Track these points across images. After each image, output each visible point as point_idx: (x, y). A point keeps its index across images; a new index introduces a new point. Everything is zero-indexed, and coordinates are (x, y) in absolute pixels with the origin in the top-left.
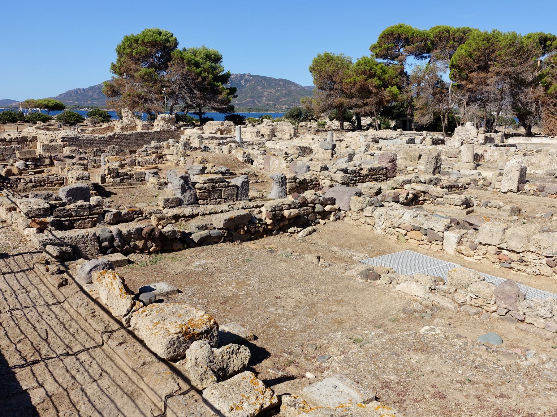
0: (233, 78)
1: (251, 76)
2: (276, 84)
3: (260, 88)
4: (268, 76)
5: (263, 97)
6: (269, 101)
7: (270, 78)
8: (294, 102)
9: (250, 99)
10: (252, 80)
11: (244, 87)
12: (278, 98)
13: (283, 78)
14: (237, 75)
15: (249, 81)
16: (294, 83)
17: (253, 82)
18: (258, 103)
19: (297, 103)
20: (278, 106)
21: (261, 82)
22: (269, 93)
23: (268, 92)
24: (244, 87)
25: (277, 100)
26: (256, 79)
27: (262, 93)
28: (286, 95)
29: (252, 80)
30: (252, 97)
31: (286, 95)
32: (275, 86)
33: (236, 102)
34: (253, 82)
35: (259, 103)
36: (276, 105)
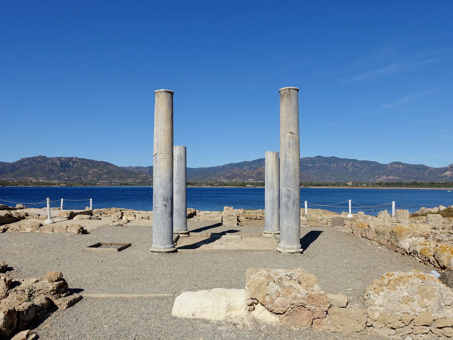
0: (63, 160)
1: (78, 159)
2: (98, 165)
3: (85, 168)
6: (93, 178)
7: (93, 161)
8: (114, 178)
9: (78, 176)
10: (78, 162)
11: (72, 167)
12: (100, 175)
13: (104, 161)
14: (66, 158)
15: (76, 162)
16: (112, 165)
17: (79, 163)
18: (83, 179)
21: (86, 163)
22: (93, 171)
24: (72, 167)
25: (100, 177)
26: (82, 161)
27: (87, 172)
28: (107, 173)
29: (78, 162)
30: (79, 175)
31: (107, 173)
32: (97, 166)
33: (66, 178)
34: (79, 163)
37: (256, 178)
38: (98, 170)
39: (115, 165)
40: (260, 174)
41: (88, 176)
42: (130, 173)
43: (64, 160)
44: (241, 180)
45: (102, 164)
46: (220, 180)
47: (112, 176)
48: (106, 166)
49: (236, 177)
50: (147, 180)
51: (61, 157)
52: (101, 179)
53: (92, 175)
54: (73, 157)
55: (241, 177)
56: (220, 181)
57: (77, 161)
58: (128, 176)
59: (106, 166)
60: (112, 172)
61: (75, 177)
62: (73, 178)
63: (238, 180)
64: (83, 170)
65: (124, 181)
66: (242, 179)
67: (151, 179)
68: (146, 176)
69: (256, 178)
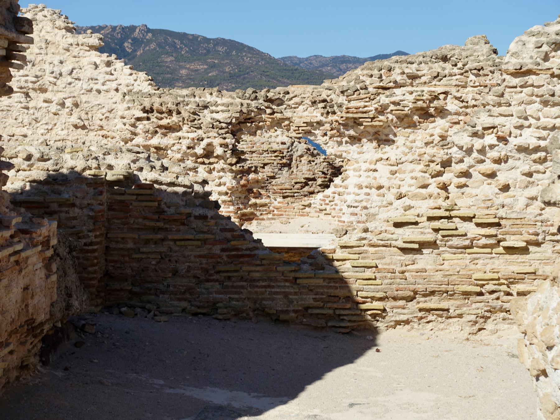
1: (149, 30)
2: (208, 51)
4: (190, 30)
5: (177, 80)
7: (195, 37)
10: (149, 41)
13: (227, 37)
14: (114, 28)
16: (251, 50)
17: (153, 46)
21: (174, 45)
22: (192, 70)
29: (149, 41)
34: (153, 46)
38: (206, 67)
39: (261, 50)
42: (307, 77)
43: (108, 34)
45: (220, 49)
48: (234, 53)
51: (101, 25)
54: (134, 25)
57: (147, 37)
59: (234, 53)
60: (247, 74)
64: (161, 67)
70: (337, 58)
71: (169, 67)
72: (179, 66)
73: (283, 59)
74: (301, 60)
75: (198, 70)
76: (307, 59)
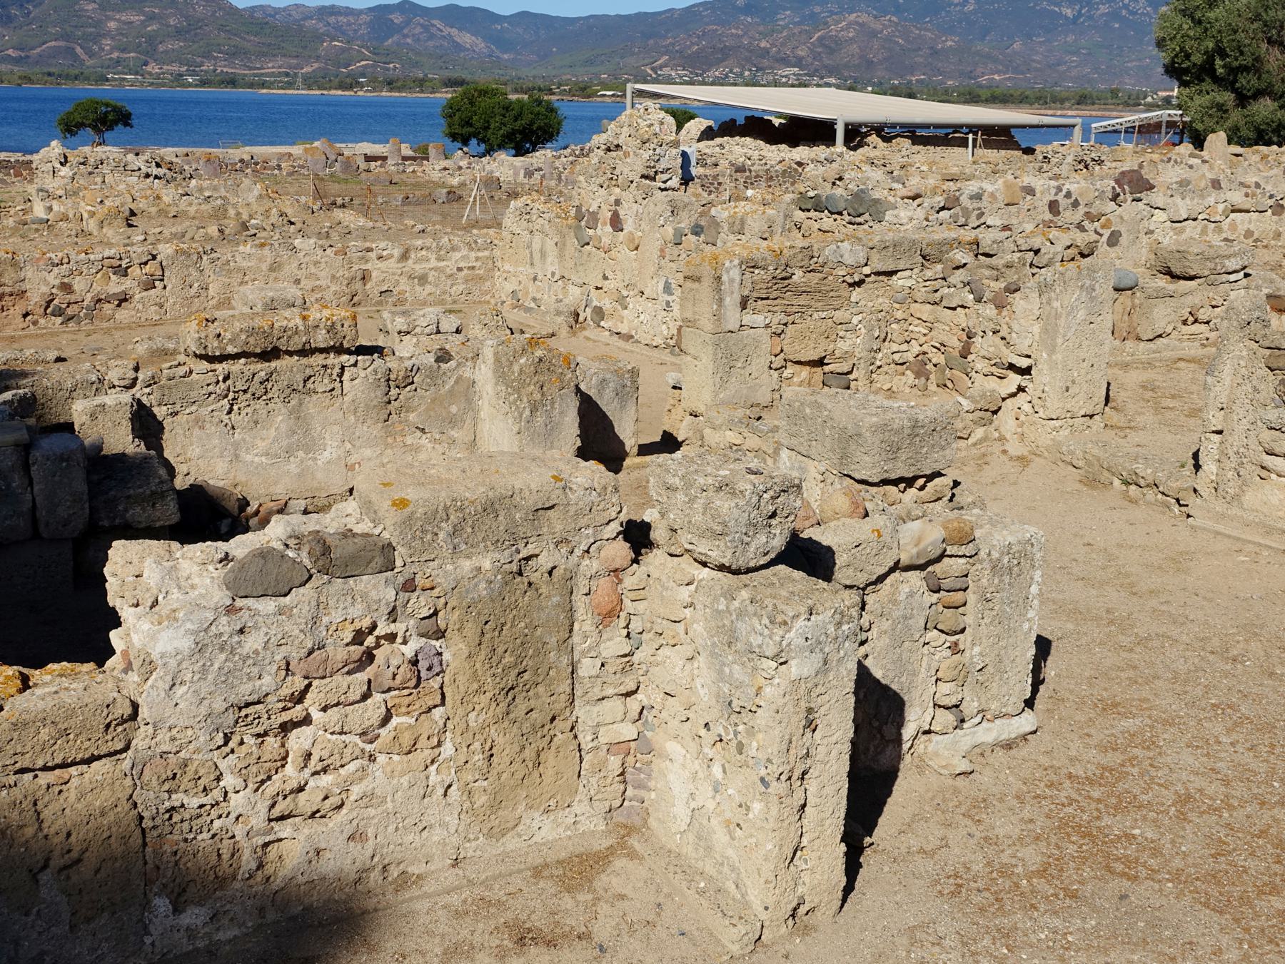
3: (90, 7)
5: (104, 36)
6: (123, 51)
8: (207, 55)
12: (152, 40)
18: (83, 56)
19: (216, 58)
20: (153, 68)
22: (125, 23)
23: (118, 20)
25: (149, 49)
27: (98, 24)
28: (179, 33)
30: (66, 37)
31: (179, 33)
33: (10, 52)
35: (91, 55)
36: (146, 64)
37: (812, 64)
38: (142, 18)
40: (830, 48)
41: (104, 42)
44: (747, 73)
46: (656, 73)
47: (201, 43)
49: (723, 60)
50: (349, 65)
52: (156, 57)
53: (120, 40)
55: (748, 60)
56: (654, 76)
58: (270, 45)
60: (200, 28)
61: (51, 47)
62: (39, 50)
63: (731, 72)
65: (251, 69)
66: (750, 70)
67: (363, 63)
68: (343, 50)
69: (812, 64)
70: (324, 8)
71: (92, 18)
72: (106, 16)
73: (253, 9)
74: (277, 11)
75: (132, 23)
76: (285, 9)
